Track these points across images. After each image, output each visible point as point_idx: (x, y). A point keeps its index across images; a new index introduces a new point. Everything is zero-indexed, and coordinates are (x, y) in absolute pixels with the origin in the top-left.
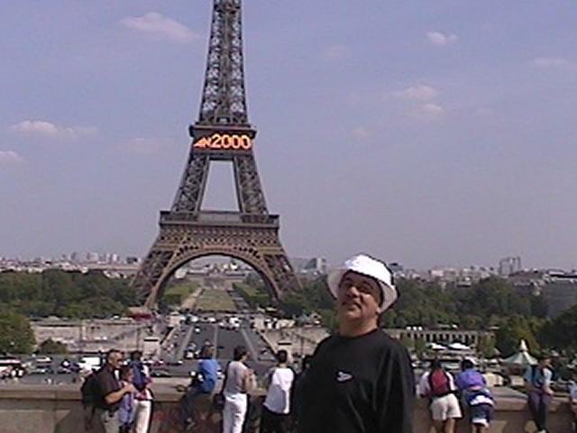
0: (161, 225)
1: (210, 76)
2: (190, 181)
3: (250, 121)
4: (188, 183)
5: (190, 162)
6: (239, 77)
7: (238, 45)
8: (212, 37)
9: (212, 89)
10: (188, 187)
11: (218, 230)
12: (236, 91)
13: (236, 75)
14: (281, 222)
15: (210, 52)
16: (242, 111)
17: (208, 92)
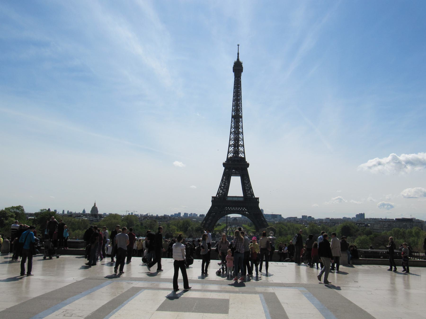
0: (212, 201)
1: (231, 143)
2: (224, 184)
3: (247, 160)
4: (223, 185)
5: (223, 177)
6: (242, 144)
7: (241, 131)
8: (231, 128)
9: (231, 149)
10: (223, 187)
11: (236, 204)
12: (241, 149)
13: (241, 143)
14: (260, 200)
15: (230, 134)
16: (243, 156)
17: (230, 150)
